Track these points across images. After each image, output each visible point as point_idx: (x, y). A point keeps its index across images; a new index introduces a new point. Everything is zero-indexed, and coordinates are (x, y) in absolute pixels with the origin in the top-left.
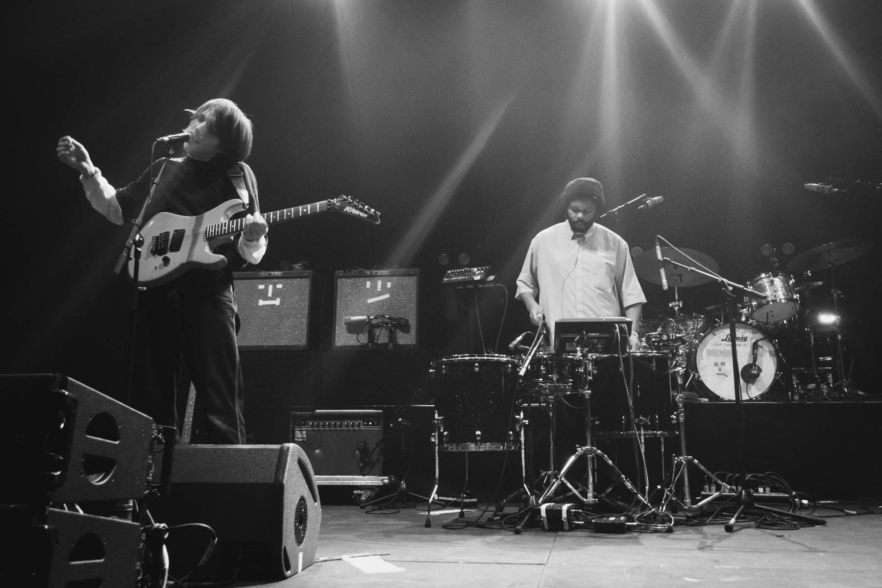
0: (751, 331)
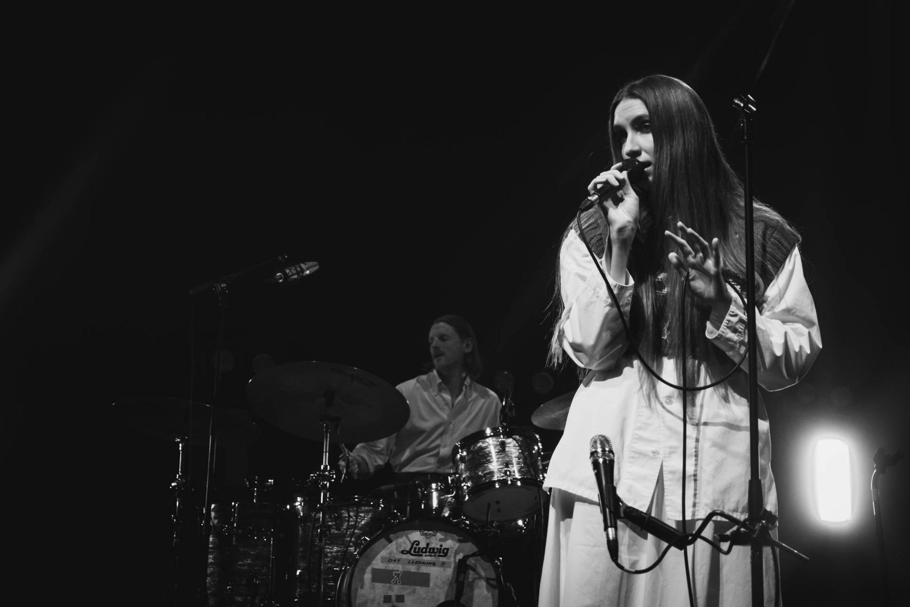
0: (456, 537)
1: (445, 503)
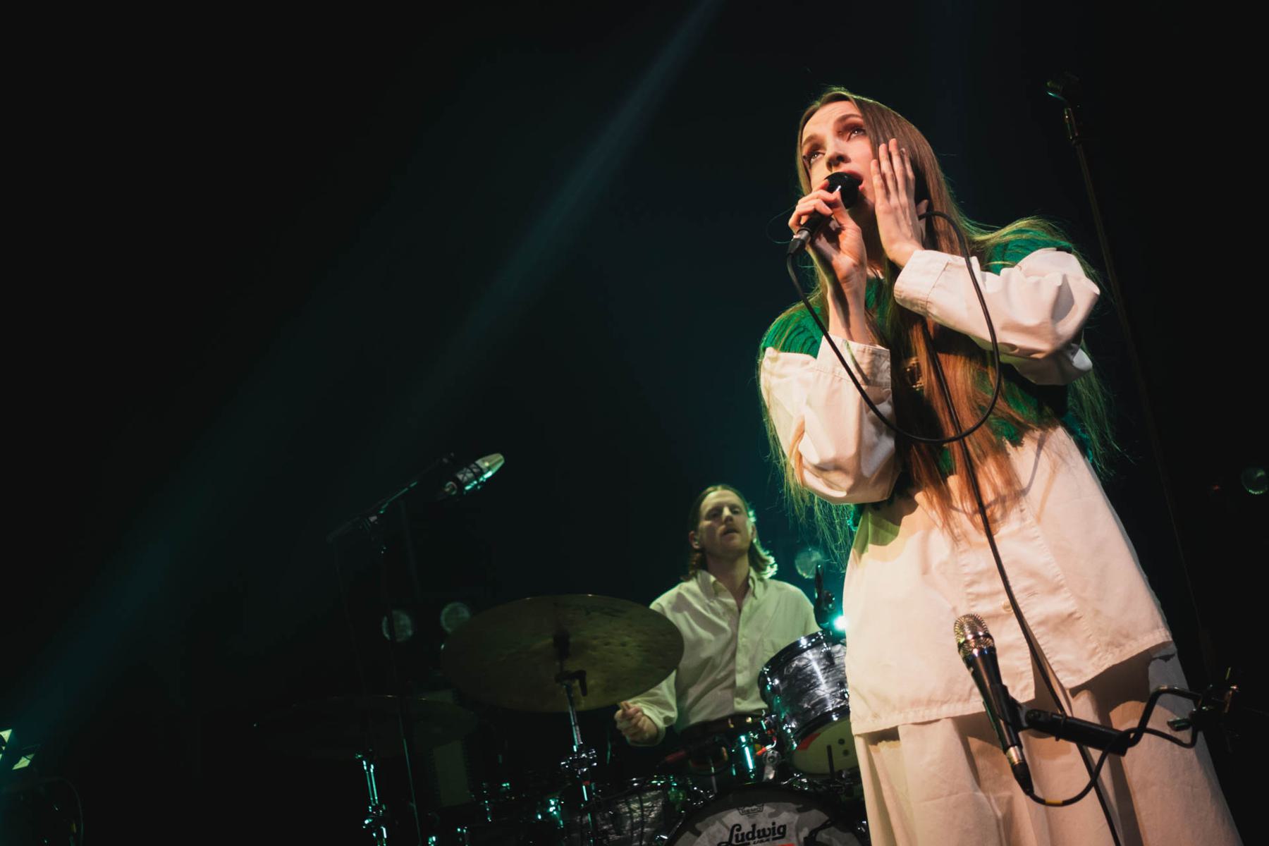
0: (793, 806)
1: (765, 760)
